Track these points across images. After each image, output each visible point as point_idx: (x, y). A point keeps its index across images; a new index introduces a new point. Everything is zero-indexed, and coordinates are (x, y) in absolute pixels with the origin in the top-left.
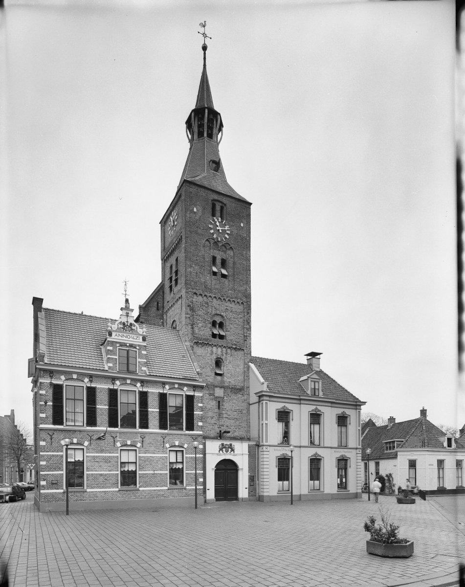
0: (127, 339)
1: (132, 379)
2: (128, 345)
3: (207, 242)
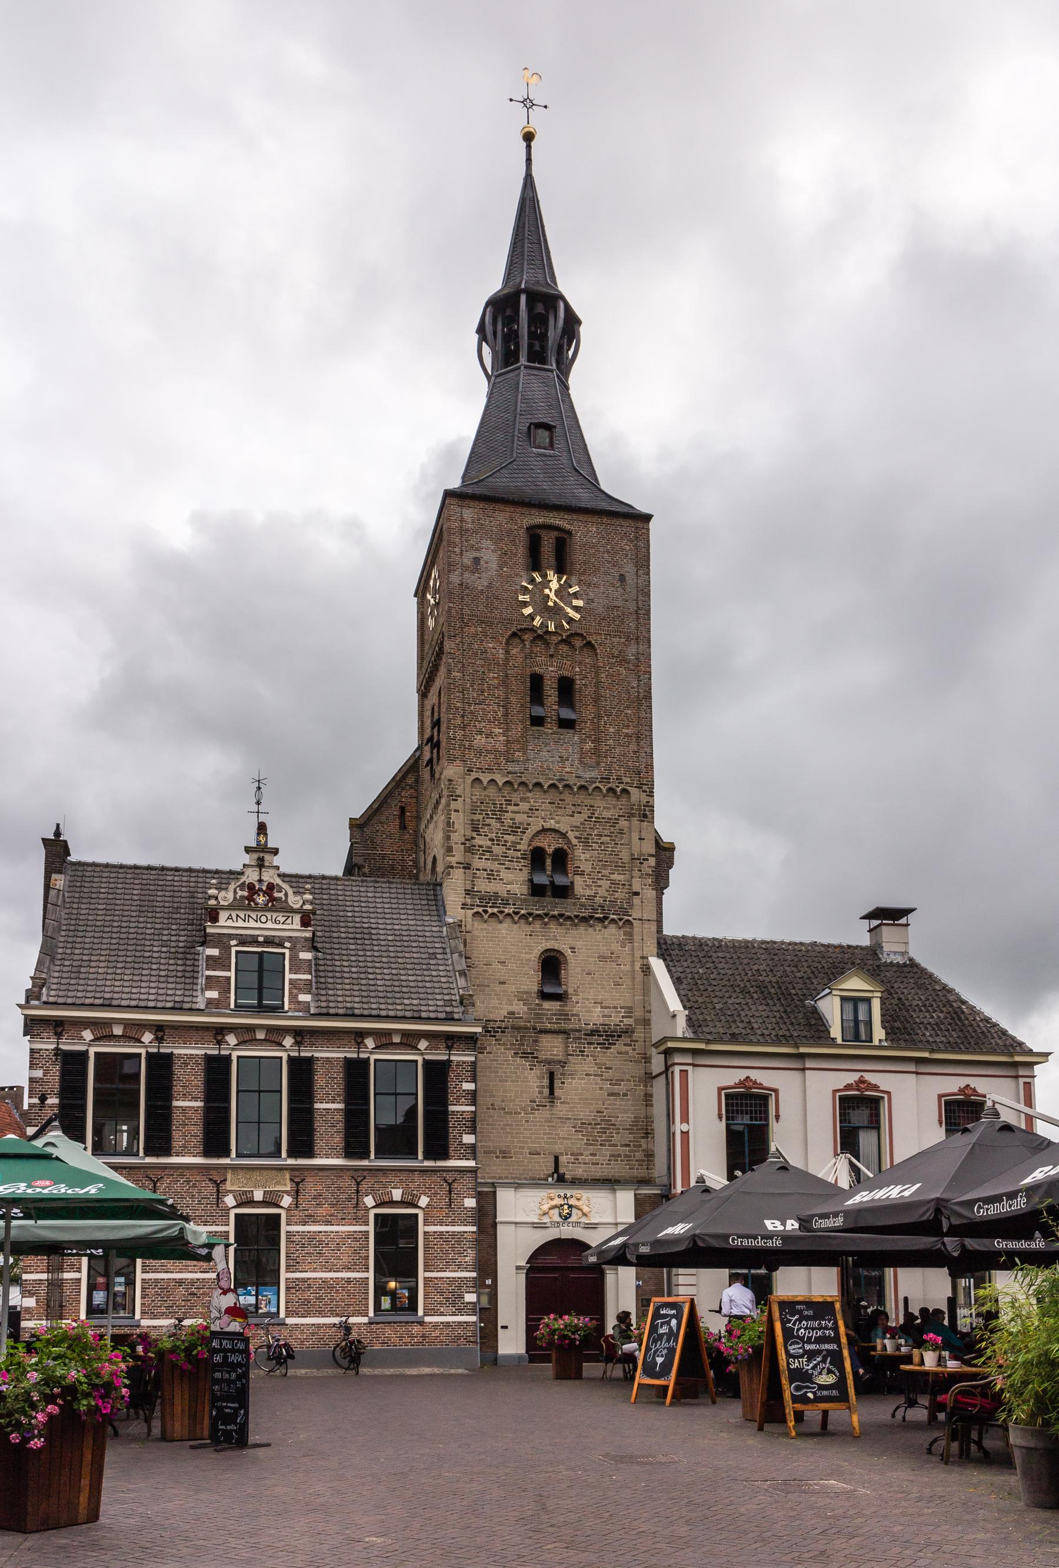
0: (259, 925)
1: (270, 1029)
2: (261, 939)
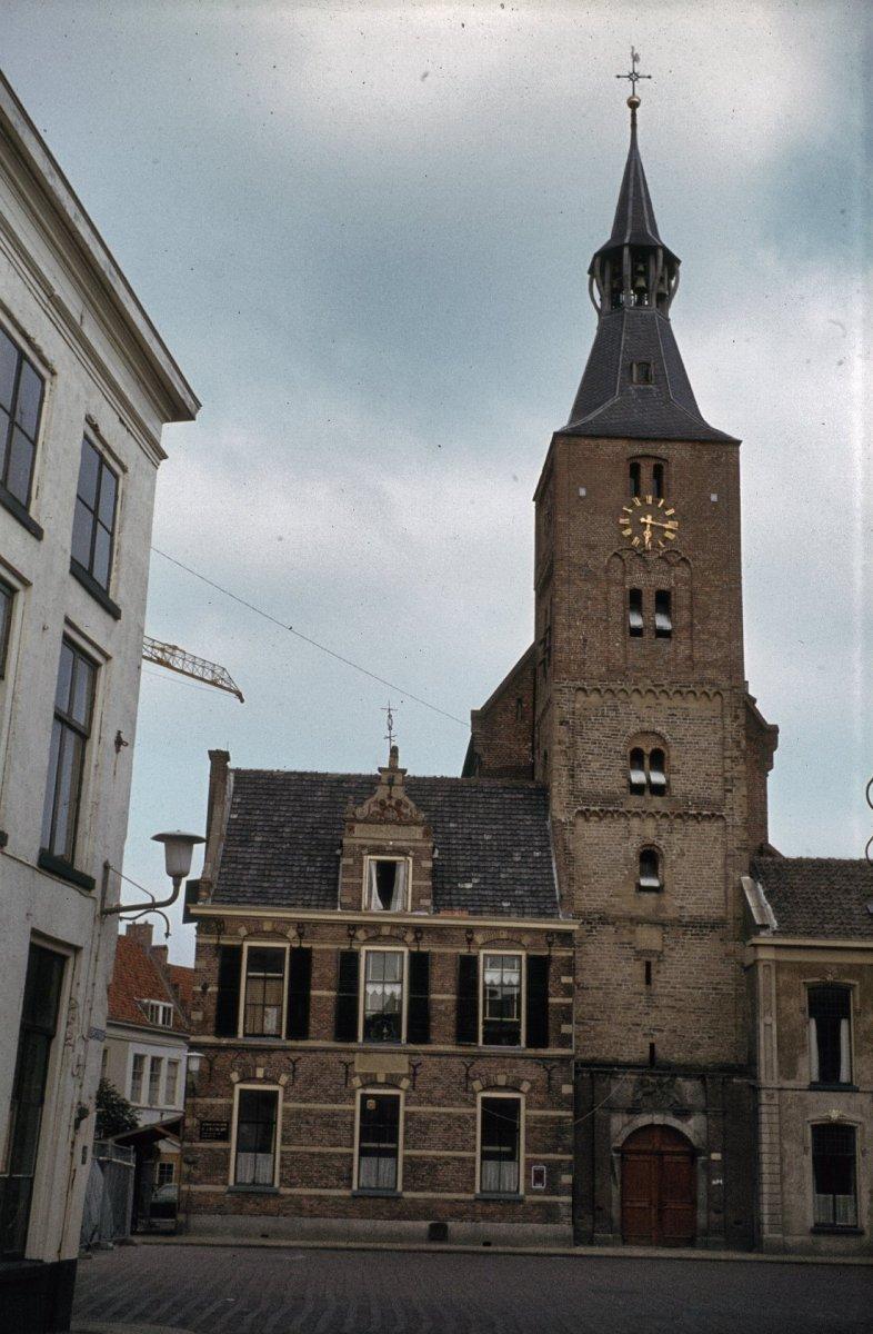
3: (617, 560)
